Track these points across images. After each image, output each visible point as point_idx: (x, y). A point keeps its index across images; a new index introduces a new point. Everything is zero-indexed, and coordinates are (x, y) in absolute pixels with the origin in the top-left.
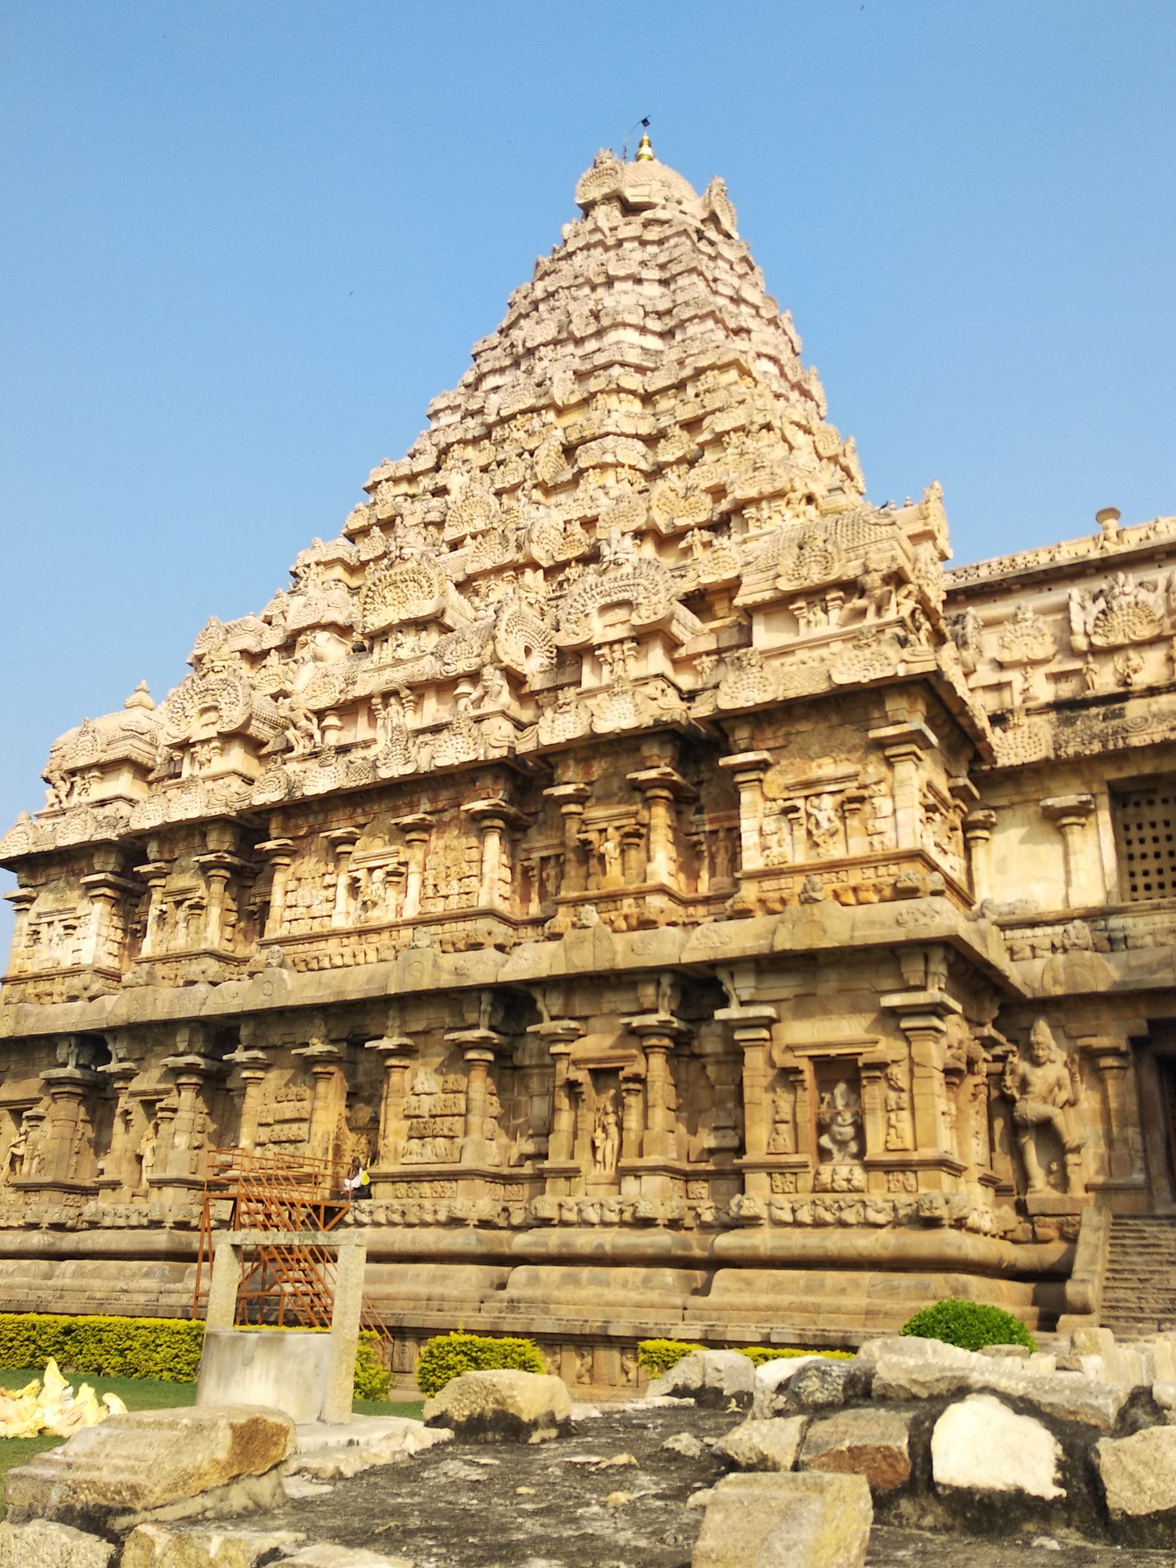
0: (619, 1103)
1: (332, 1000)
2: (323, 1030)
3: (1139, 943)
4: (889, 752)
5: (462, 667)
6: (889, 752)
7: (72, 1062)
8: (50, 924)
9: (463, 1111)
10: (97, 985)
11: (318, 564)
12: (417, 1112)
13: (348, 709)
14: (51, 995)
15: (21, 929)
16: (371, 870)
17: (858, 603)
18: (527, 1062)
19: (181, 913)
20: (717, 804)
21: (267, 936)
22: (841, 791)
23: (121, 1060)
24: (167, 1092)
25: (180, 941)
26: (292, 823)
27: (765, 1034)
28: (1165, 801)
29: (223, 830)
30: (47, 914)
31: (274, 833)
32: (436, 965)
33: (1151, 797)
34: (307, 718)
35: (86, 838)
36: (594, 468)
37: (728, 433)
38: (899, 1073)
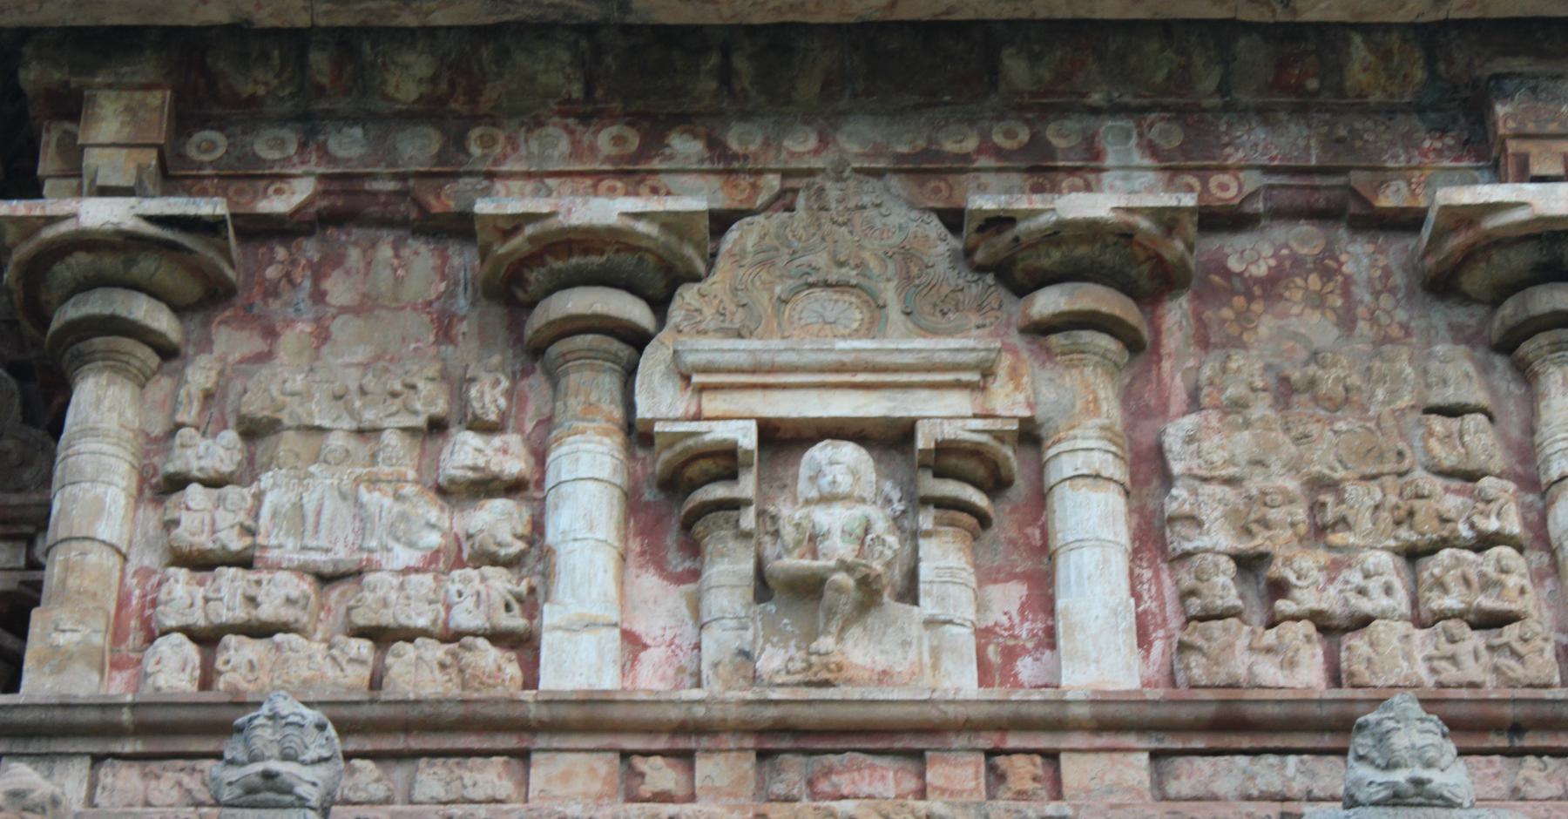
16: (783, 440)
26: (208, 147)
31: (106, 164)
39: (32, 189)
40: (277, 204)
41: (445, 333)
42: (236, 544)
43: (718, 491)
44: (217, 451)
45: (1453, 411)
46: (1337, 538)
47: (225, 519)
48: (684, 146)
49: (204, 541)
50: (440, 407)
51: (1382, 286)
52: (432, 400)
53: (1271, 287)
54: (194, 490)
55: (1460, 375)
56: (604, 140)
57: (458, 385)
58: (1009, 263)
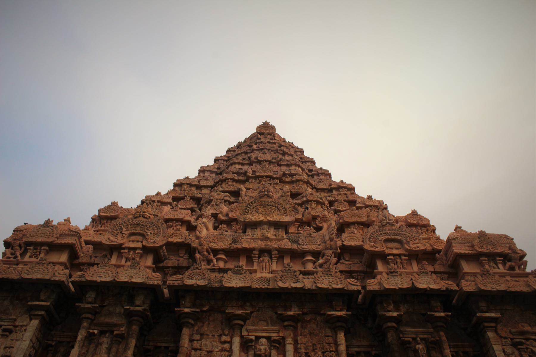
13: (233, 254)
16: (258, 338)
17: (508, 264)
19: (105, 340)
34: (208, 251)
35: (47, 277)
39: (180, 307)
40: (205, 309)
41: (222, 324)
42: (199, 348)
43: (250, 344)
44: (197, 337)
45: (328, 336)
46: (316, 351)
47: (198, 345)
48: (248, 304)
49: (196, 347)
50: (221, 333)
52: (220, 332)
53: (309, 322)
54: (195, 342)
55: (329, 333)
56: (239, 303)
57: (223, 330)
58: (282, 319)
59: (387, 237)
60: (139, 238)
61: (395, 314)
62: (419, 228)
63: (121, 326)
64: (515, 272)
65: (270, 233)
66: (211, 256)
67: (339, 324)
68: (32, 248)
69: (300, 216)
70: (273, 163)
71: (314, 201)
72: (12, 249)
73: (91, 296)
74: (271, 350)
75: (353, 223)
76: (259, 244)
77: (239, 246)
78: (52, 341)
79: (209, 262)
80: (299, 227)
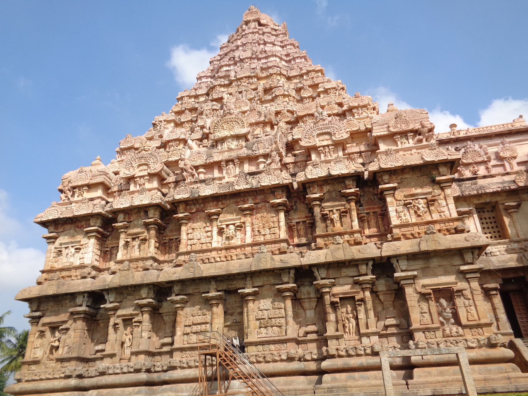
0: (355, 309)
1: (224, 273)
2: (215, 287)
3: (496, 254)
4: (442, 185)
5: (261, 152)
6: (442, 185)
7: (84, 304)
8: (66, 248)
9: (284, 315)
10: (94, 273)
11: (165, 121)
12: (263, 317)
13: (209, 167)
14: (71, 276)
15: (51, 250)
16: (227, 226)
17: (418, 137)
18: (303, 297)
19: (136, 243)
20: (368, 203)
21: (181, 250)
22: (426, 198)
23: (111, 303)
24: (137, 315)
25: (136, 254)
26: (188, 207)
27: (412, 281)
28: (488, 211)
29: (155, 210)
30: (65, 244)
31: (182, 211)
32: (272, 259)
33: (484, 210)
34: (191, 169)
35: (90, 212)
36: (281, 95)
37: (329, 89)
38: (467, 293)
40: (193, 211)
48: (220, 203)
51: (269, 207)
53: (261, 208)
59: (319, 132)
60: (145, 167)
61: (317, 195)
62: (360, 109)
63: (143, 233)
64: (423, 144)
65: (234, 144)
66: (194, 172)
67: (281, 208)
68: (77, 190)
69: (262, 119)
70: (254, 59)
71: (281, 95)
72: (65, 193)
73: (121, 217)
74: (236, 232)
75: (305, 116)
76: (226, 156)
77: (212, 161)
78: (107, 248)
79: (193, 176)
80: (264, 126)
